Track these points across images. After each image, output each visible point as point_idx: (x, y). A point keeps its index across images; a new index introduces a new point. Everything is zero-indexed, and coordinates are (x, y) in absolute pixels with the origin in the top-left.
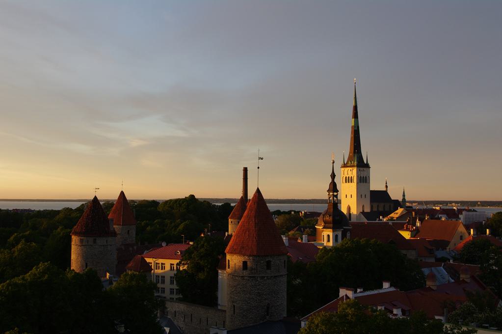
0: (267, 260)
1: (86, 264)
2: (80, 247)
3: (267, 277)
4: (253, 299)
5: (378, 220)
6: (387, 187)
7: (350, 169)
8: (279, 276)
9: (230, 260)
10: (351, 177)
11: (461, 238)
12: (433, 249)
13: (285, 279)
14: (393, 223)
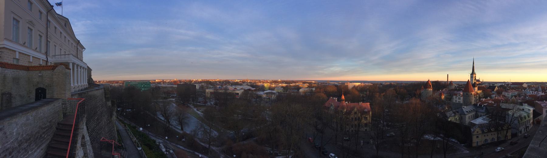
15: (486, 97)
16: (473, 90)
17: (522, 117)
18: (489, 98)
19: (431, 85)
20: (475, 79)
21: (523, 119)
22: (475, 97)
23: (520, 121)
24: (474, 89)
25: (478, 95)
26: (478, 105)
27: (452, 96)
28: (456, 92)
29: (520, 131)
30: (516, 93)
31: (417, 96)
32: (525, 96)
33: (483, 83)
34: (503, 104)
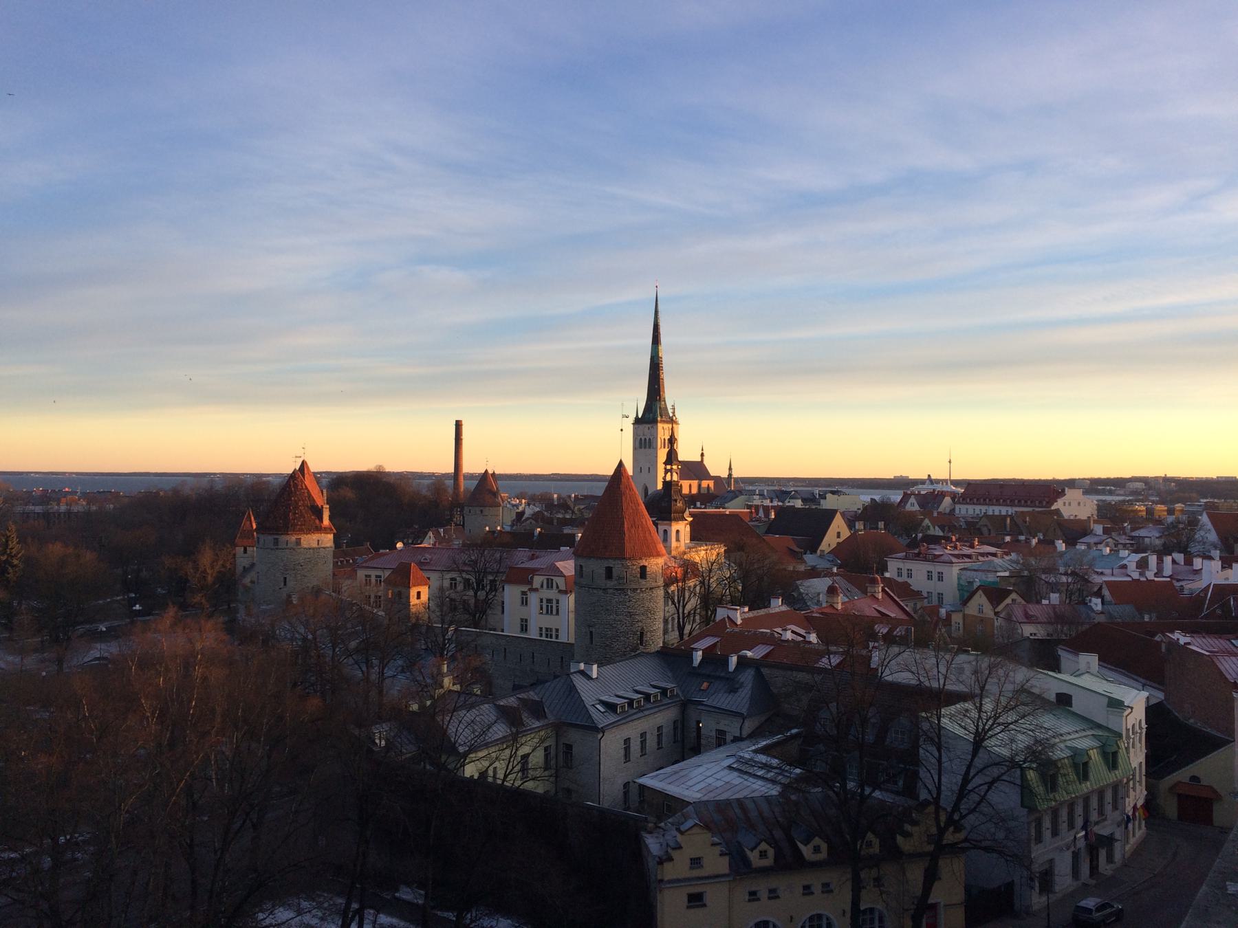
4: (621, 621)
5: (693, 508)
6: (702, 455)
7: (647, 426)
10: (650, 439)
11: (839, 535)
12: (801, 553)
15: (756, 599)
16: (659, 538)
17: (1053, 763)
18: (777, 605)
19: (320, 500)
20: (672, 457)
21: (1061, 780)
22: (668, 596)
23: (1040, 790)
24: (665, 531)
25: (691, 583)
26: (698, 656)
27: (494, 587)
28: (521, 557)
29: (1036, 868)
30: (1003, 565)
31: (198, 598)
32: (1081, 587)
33: (729, 488)
34: (895, 649)
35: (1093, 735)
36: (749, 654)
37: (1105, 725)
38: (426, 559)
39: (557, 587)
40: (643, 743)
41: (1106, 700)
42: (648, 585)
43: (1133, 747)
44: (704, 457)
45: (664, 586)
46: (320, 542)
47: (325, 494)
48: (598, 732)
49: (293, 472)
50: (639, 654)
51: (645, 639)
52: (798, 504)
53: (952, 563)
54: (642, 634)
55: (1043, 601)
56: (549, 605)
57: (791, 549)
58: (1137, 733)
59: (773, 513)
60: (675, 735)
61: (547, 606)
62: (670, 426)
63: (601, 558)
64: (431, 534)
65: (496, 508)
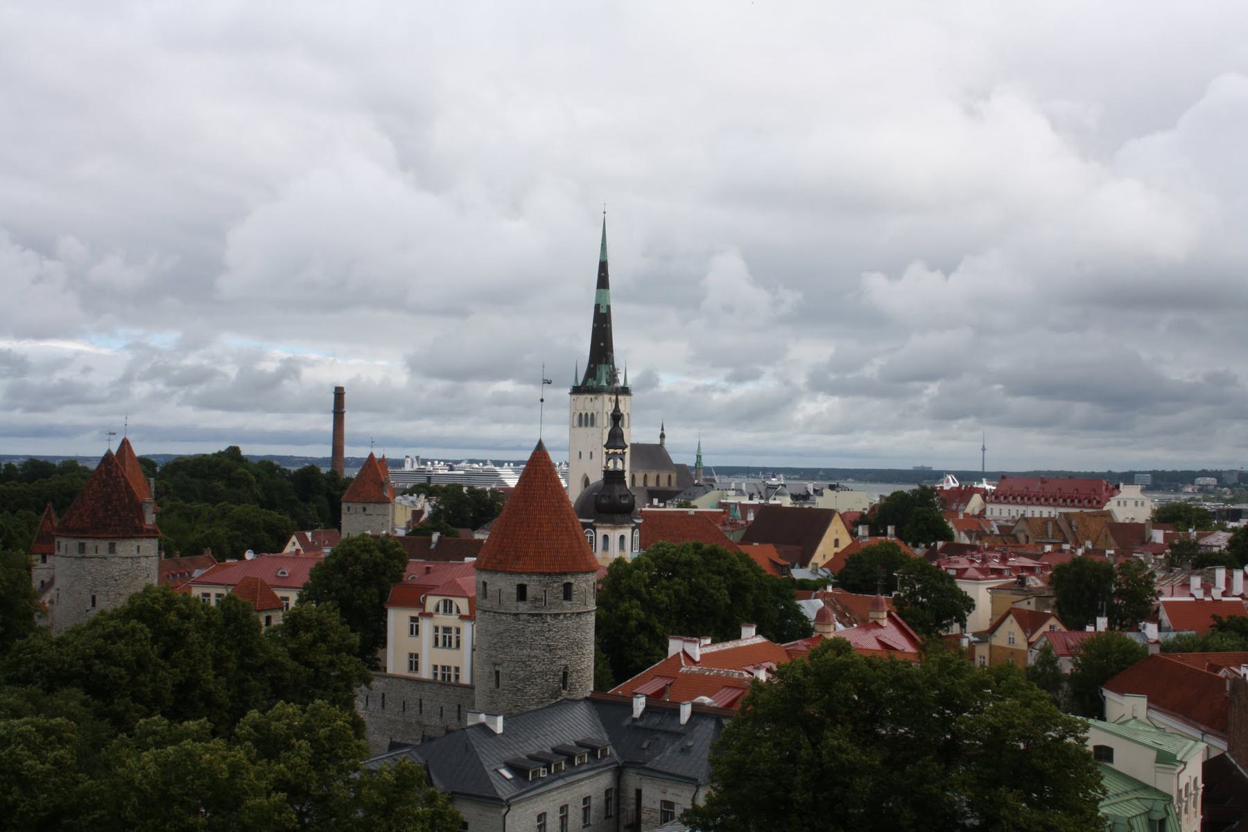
0: (565, 581)
1: (94, 598)
2: (78, 562)
3: (566, 614)
5: (649, 507)
6: (662, 436)
7: (589, 397)
8: (585, 612)
9: (488, 582)
10: (592, 414)
11: (836, 543)
12: (787, 566)
13: (592, 619)
14: (695, 512)
24: (606, 537)
35: (1137, 798)
36: (706, 700)
37: (1151, 784)
38: (284, 573)
39: (458, 611)
40: (564, 819)
41: (1153, 754)
42: (575, 610)
43: (1186, 812)
44: (666, 441)
45: (596, 610)
46: (140, 550)
47: (153, 485)
48: (503, 807)
49: (106, 455)
50: (562, 701)
51: (569, 681)
52: (787, 502)
53: (978, 579)
54: (565, 674)
55: (1087, 627)
56: (447, 635)
57: (774, 563)
58: (1191, 795)
59: (752, 514)
60: (607, 809)
61: (445, 637)
62: (614, 397)
63: (511, 573)
64: (294, 539)
65: (386, 505)
